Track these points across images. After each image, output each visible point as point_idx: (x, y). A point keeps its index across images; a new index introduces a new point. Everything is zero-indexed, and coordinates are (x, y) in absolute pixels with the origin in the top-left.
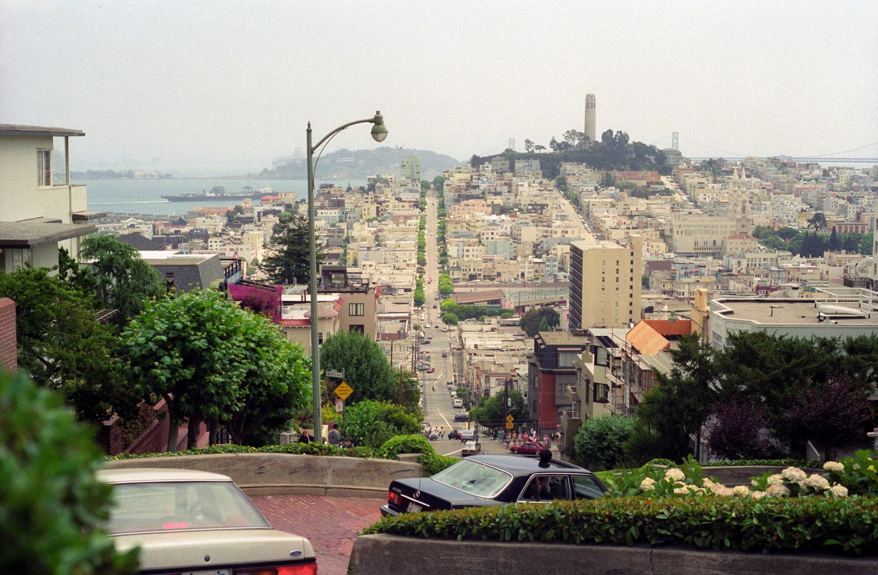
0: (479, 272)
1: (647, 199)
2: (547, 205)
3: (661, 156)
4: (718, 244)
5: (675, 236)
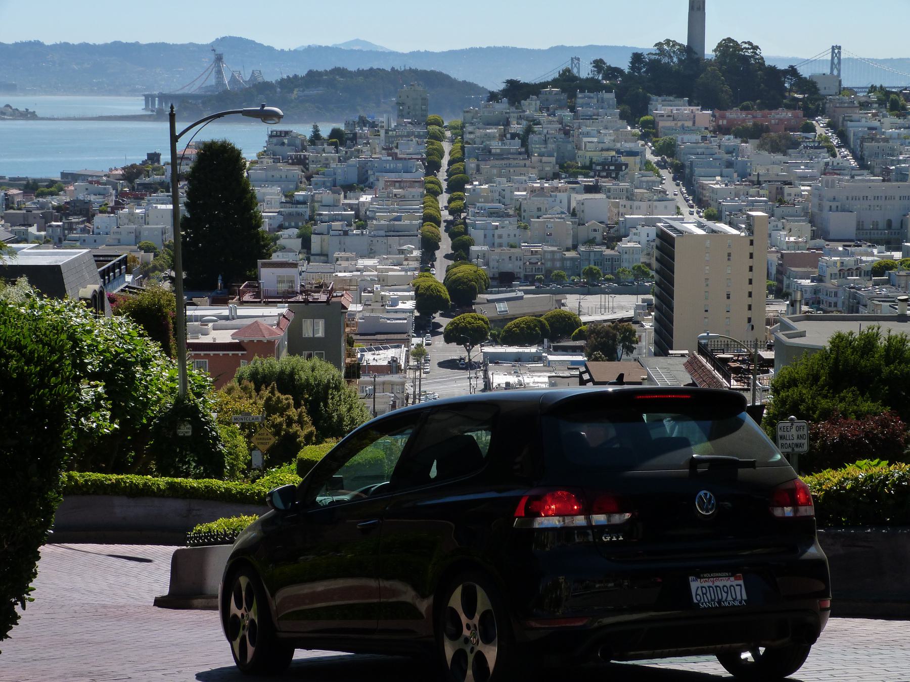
1: (785, 154)
3: (808, 86)
4: (896, 225)
5: (826, 214)
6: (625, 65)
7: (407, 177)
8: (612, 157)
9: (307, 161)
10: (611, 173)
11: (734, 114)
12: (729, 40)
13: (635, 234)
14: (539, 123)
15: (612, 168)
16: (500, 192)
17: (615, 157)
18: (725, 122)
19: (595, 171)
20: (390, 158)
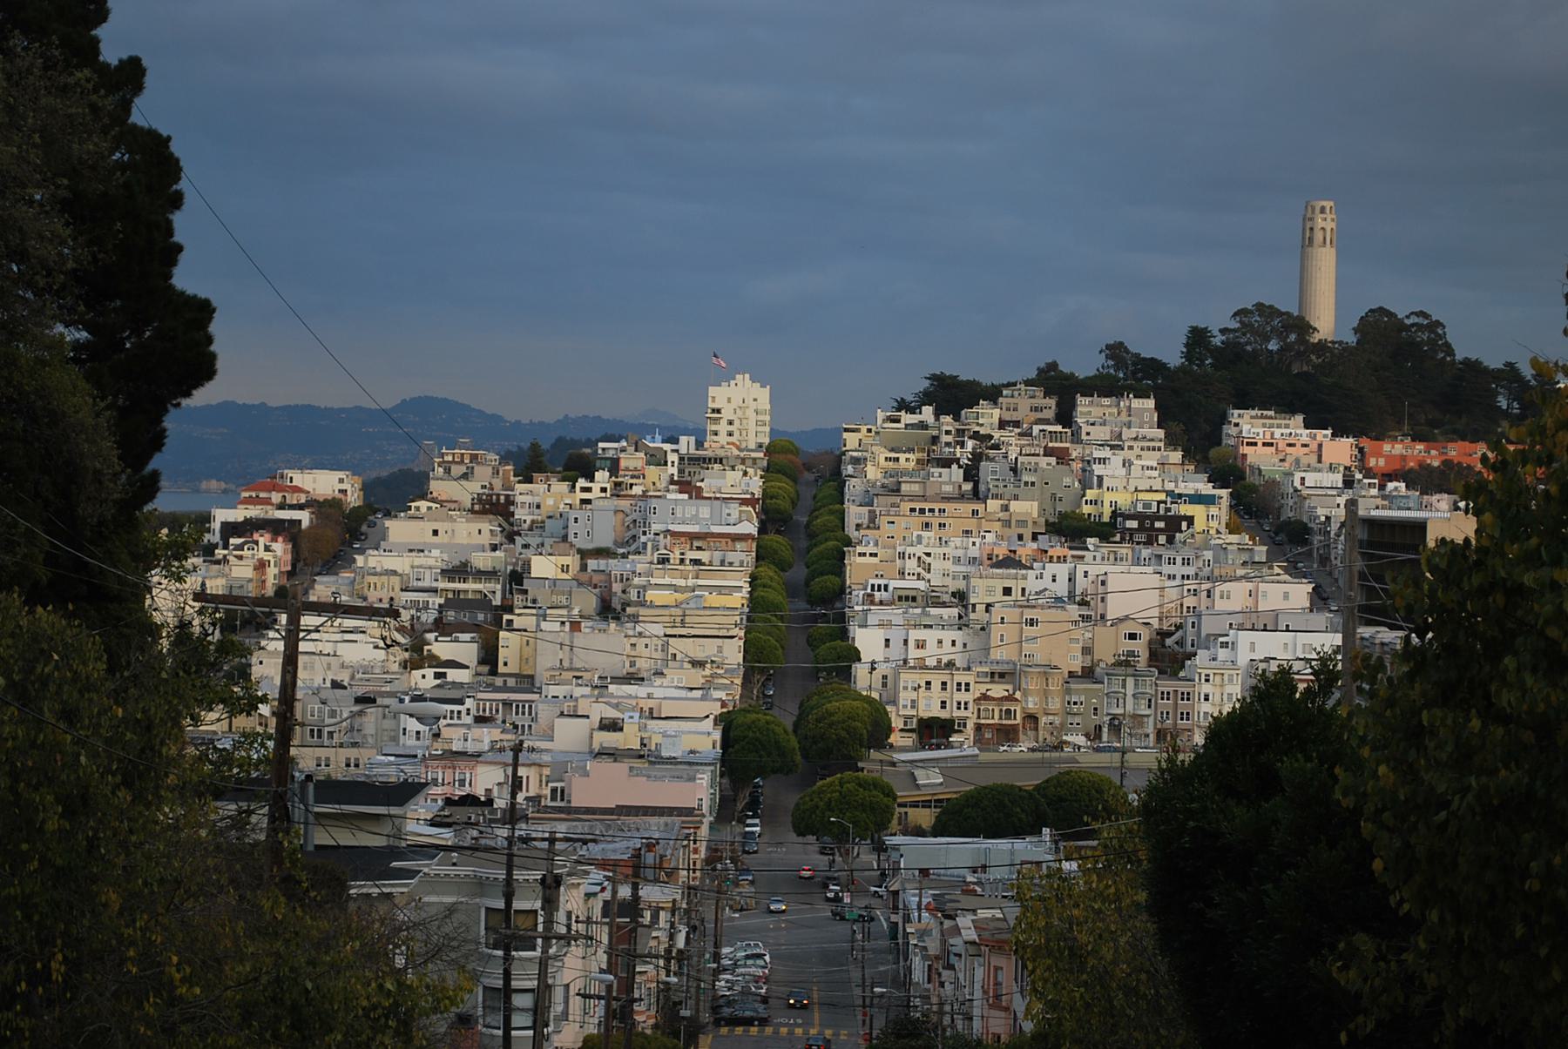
0: (962, 713)
2: (1190, 520)
6: (1172, 354)
7: (715, 529)
8: (1159, 502)
9: (512, 508)
10: (1157, 536)
11: (1396, 449)
12: (1381, 309)
13: (1225, 645)
14: (996, 447)
15: (1160, 525)
16: (919, 558)
17: (1165, 502)
18: (1382, 462)
19: (1124, 531)
20: (686, 496)
